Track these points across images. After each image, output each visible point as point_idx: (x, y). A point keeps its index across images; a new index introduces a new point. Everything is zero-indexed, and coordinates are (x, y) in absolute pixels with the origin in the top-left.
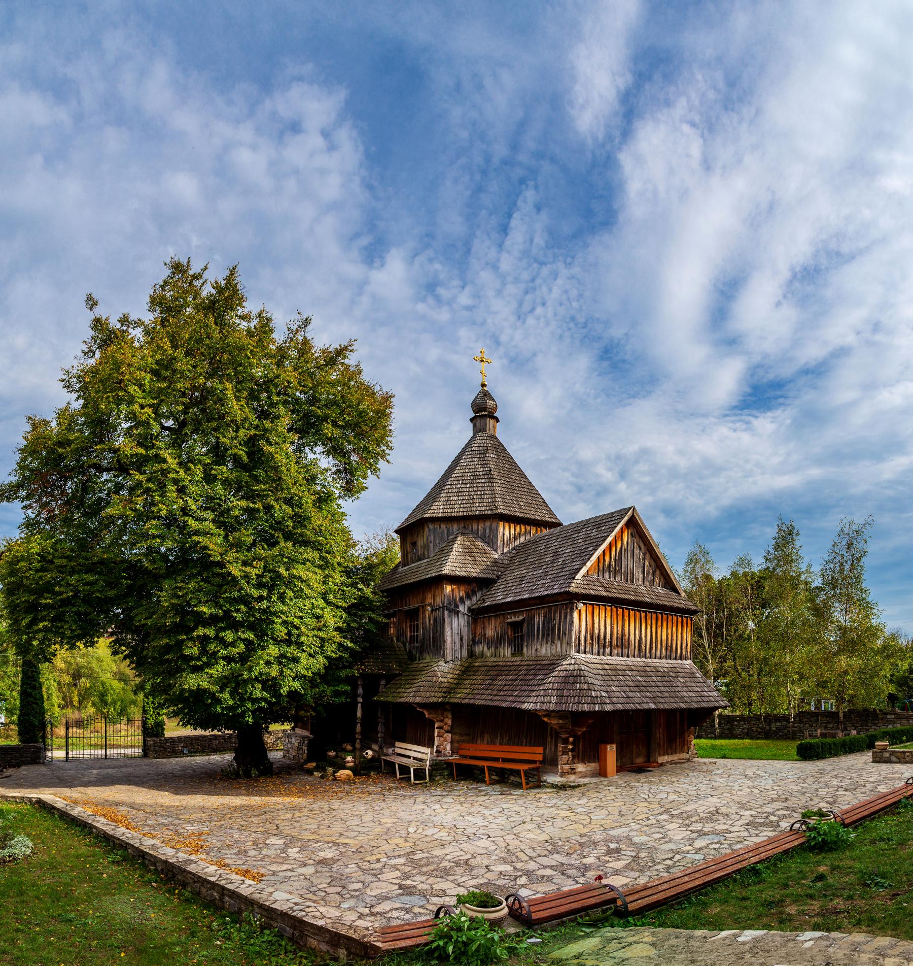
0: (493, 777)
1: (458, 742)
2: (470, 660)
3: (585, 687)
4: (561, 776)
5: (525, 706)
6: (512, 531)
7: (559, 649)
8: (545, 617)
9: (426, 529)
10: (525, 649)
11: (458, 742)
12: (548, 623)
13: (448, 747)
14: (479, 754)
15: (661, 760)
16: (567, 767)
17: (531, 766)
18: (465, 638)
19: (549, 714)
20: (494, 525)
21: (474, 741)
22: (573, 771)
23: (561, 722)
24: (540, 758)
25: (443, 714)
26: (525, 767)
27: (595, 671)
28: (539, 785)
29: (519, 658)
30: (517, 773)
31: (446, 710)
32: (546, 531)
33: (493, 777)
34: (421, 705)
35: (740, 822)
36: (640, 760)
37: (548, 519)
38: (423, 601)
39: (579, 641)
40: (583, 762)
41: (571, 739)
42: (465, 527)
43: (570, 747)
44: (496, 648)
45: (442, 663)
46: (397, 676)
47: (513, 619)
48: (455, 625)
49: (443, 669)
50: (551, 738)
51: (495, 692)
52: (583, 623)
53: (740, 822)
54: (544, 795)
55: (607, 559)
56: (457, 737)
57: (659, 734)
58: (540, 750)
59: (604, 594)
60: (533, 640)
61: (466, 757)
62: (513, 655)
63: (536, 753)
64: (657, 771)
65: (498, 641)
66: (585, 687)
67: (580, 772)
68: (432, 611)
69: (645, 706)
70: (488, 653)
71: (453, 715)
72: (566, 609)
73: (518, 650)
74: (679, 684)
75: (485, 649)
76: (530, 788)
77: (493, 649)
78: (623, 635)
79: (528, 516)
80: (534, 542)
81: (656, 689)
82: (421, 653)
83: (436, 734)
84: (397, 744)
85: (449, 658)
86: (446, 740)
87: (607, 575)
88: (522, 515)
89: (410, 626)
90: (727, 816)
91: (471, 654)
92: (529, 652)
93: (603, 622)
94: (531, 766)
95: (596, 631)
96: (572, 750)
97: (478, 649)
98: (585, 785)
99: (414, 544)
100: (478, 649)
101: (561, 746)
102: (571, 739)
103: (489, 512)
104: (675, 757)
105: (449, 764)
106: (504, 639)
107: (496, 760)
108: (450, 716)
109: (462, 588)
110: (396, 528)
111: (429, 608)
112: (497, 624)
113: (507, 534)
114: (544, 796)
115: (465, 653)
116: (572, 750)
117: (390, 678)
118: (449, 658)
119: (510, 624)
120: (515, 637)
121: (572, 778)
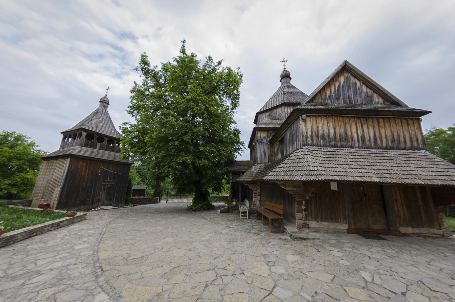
3: (306, 164)
16: (301, 222)
22: (306, 226)
23: (294, 189)
27: (316, 155)
40: (316, 219)
41: (304, 202)
43: (304, 207)
45: (256, 165)
46: (246, 172)
48: (262, 148)
58: (281, 207)
66: (306, 164)
67: (314, 228)
78: (346, 133)
91: (270, 160)
93: (325, 126)
95: (321, 132)
96: (305, 210)
102: (304, 202)
109: (266, 133)
113: (289, 111)
115: (267, 160)
116: (305, 210)
121: (307, 230)
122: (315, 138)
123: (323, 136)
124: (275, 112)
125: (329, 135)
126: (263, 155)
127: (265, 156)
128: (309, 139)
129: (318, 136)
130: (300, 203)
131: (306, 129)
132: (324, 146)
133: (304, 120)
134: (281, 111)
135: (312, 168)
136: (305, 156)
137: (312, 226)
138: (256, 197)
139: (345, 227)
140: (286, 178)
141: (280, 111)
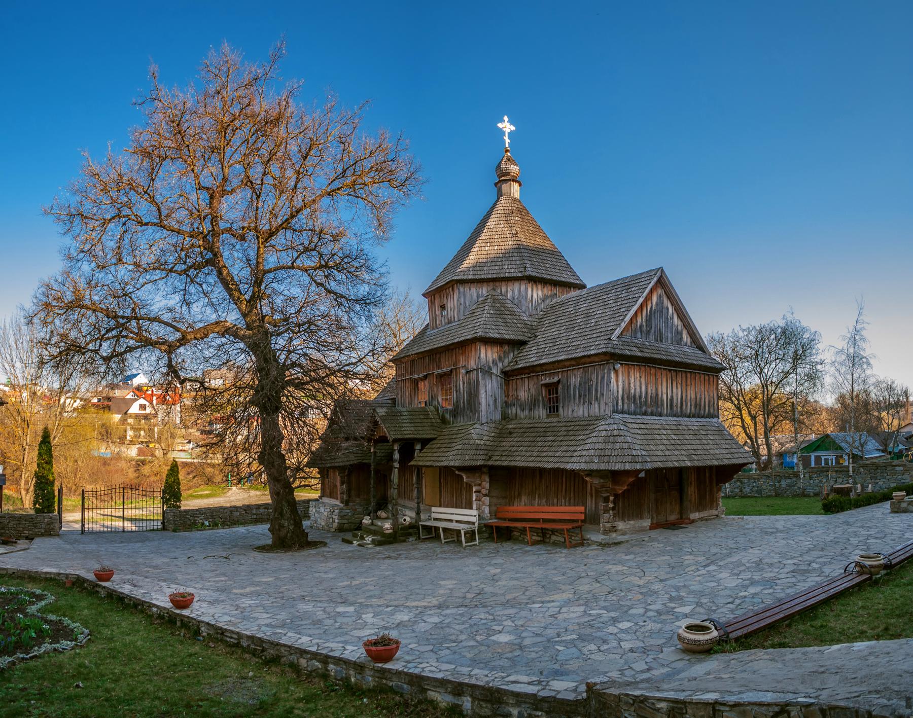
0: (534, 538)
1: (496, 505)
2: (504, 422)
3: (626, 446)
4: (604, 534)
5: (569, 466)
6: (540, 294)
7: (597, 410)
8: (582, 378)
9: (456, 291)
10: (561, 410)
11: (496, 505)
12: (585, 383)
13: (487, 510)
14: (519, 516)
15: (694, 516)
16: (608, 525)
17: (575, 525)
18: (499, 400)
19: (590, 473)
20: (523, 287)
21: (511, 503)
22: (614, 529)
23: (602, 481)
24: (582, 517)
25: (480, 477)
26: (569, 526)
28: (582, 543)
29: (555, 420)
30: (561, 532)
31: (483, 473)
32: (574, 293)
33: (534, 538)
34: (460, 469)
35: (786, 570)
36: (673, 518)
37: (572, 281)
38: (455, 364)
39: (617, 400)
41: (612, 498)
42: (494, 289)
43: (611, 505)
44: (530, 410)
47: (548, 381)
48: (489, 387)
49: (479, 433)
50: (592, 496)
51: (536, 454)
52: (620, 383)
53: (786, 570)
54: (591, 552)
55: (639, 320)
56: (495, 500)
57: (692, 492)
58: (582, 509)
59: (639, 354)
60: (569, 401)
61: (505, 519)
62: (548, 416)
63: (576, 511)
64: (691, 528)
65: (533, 404)
66: (626, 446)
68: (467, 373)
69: (683, 465)
70: (522, 415)
71: (490, 477)
72: (603, 370)
73: (553, 409)
74: (710, 442)
75: (519, 410)
76: (575, 546)
77: (527, 412)
79: (555, 278)
80: (562, 304)
81: (689, 447)
82: (455, 416)
83: (474, 498)
84: (433, 509)
85: (484, 421)
86: (484, 504)
87: (639, 335)
88: (549, 277)
89: (442, 389)
90: (771, 565)
91: (505, 417)
92: (565, 412)
94: (575, 525)
95: (632, 391)
97: (513, 411)
98: (627, 541)
99: (443, 307)
100: (513, 411)
101: (602, 505)
102: (612, 498)
103: (520, 275)
104: (705, 514)
105: (488, 527)
106: (539, 400)
107: (538, 520)
108: (488, 480)
109: (495, 349)
110: (423, 291)
111: (463, 371)
112: (531, 386)
114: (591, 553)
115: (498, 416)
116: (613, 509)
117: (425, 442)
118: (484, 421)
119: (543, 385)
120: (550, 399)
121: (614, 535)
122: (626, 401)
123: (635, 395)
124: (504, 290)
125: (640, 397)
126: (491, 403)
127: (495, 407)
128: (620, 403)
129: (629, 398)
130: (606, 500)
131: (618, 386)
132: (635, 413)
133: (616, 371)
134: (519, 291)
135: (634, 453)
136: (622, 433)
137: (620, 528)
138: (480, 500)
139: (647, 523)
140: (603, 467)
141: (516, 293)
